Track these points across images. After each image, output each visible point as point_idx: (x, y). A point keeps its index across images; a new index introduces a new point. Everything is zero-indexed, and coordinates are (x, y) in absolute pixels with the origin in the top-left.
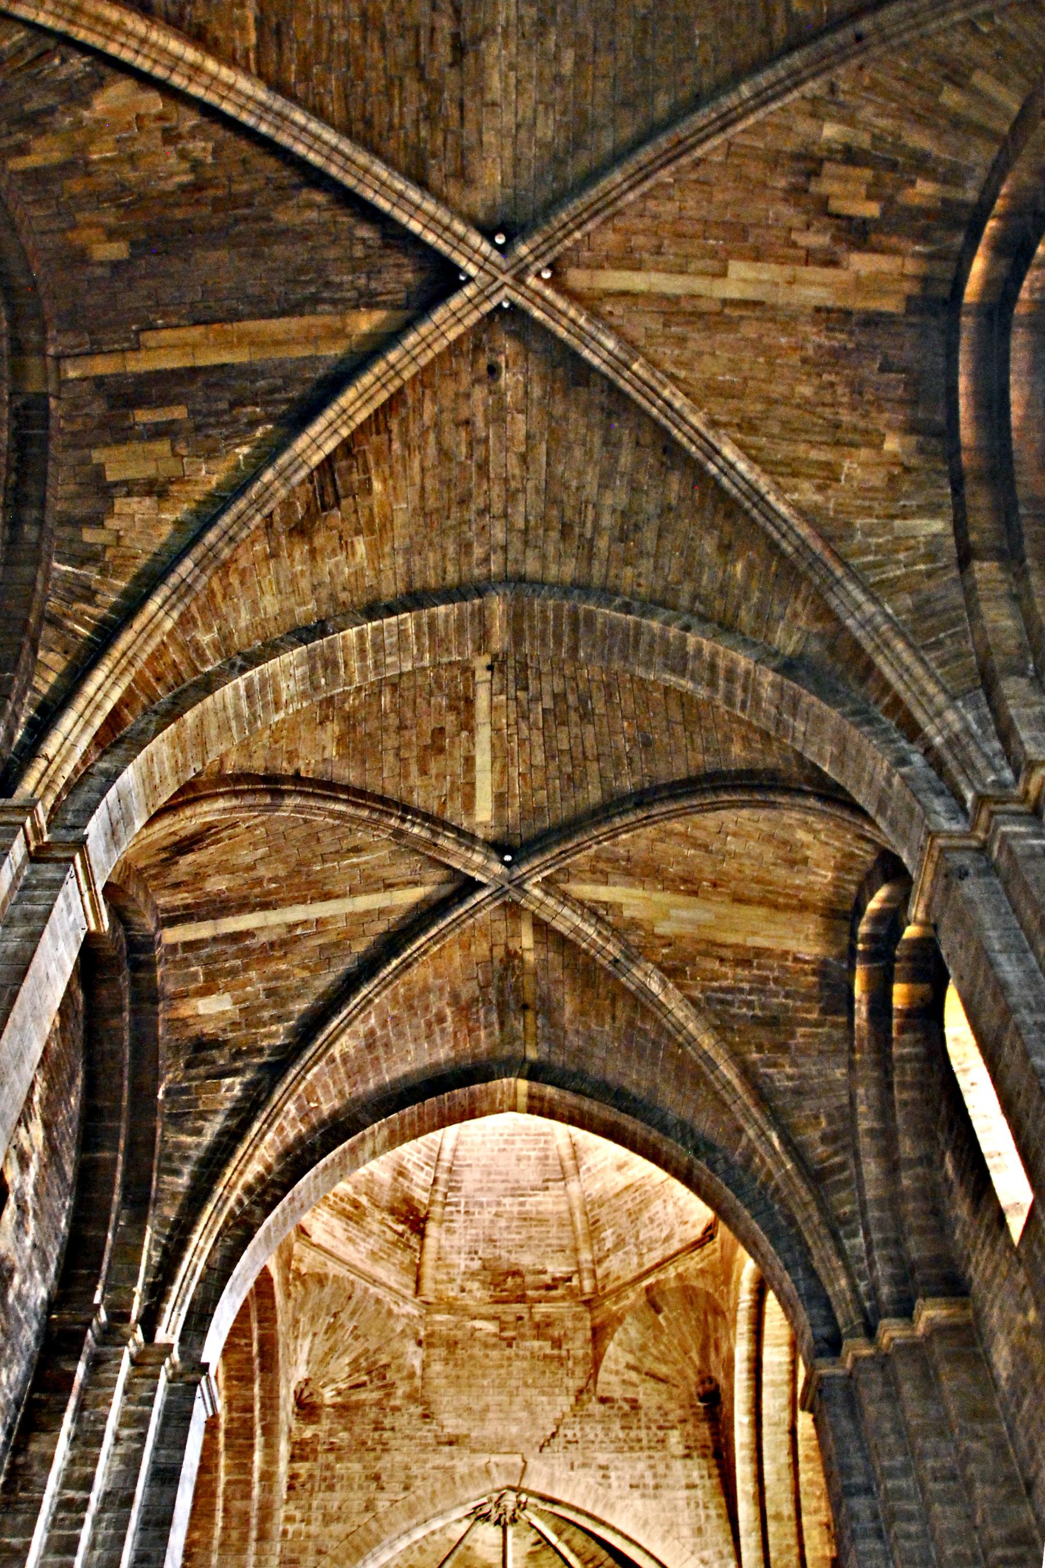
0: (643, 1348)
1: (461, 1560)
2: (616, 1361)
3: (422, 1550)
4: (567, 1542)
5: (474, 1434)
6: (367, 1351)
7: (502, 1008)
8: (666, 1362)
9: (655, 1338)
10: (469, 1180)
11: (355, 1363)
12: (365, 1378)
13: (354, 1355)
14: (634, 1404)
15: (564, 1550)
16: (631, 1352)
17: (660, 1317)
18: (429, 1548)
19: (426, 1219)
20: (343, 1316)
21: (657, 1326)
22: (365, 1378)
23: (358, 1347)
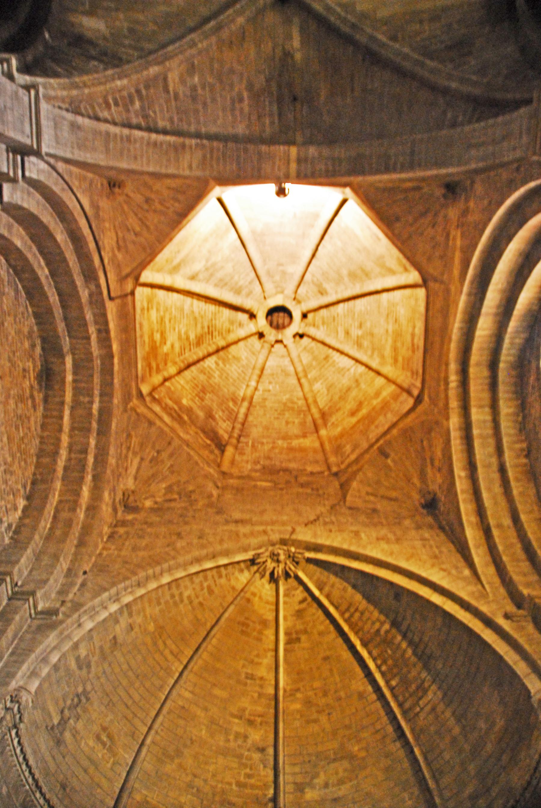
0: (378, 482)
1: (242, 611)
2: (359, 491)
3: (211, 591)
4: (328, 596)
5: (254, 519)
6: (179, 481)
7: (280, 101)
8: (395, 489)
9: (386, 475)
10: (255, 432)
11: (169, 489)
12: (176, 496)
13: (169, 483)
14: (374, 511)
15: (326, 602)
16: (369, 485)
17: (389, 461)
18: (216, 590)
19: (225, 446)
20: (164, 455)
21: (388, 467)
22: (176, 496)
23: (173, 479)
